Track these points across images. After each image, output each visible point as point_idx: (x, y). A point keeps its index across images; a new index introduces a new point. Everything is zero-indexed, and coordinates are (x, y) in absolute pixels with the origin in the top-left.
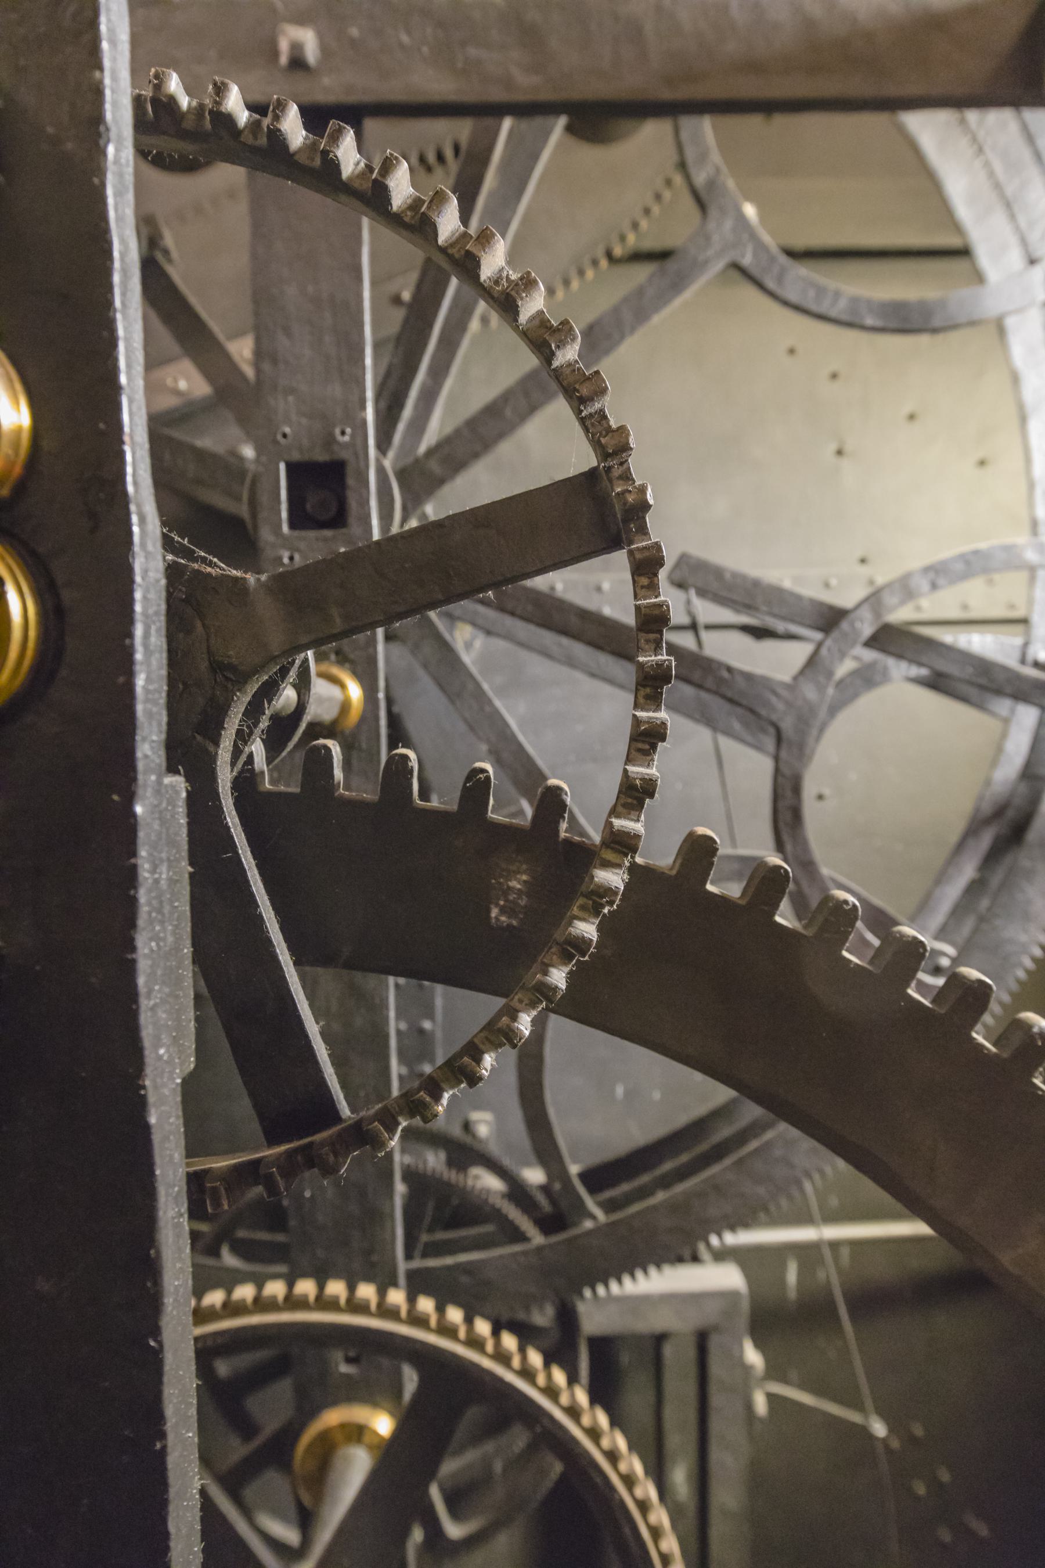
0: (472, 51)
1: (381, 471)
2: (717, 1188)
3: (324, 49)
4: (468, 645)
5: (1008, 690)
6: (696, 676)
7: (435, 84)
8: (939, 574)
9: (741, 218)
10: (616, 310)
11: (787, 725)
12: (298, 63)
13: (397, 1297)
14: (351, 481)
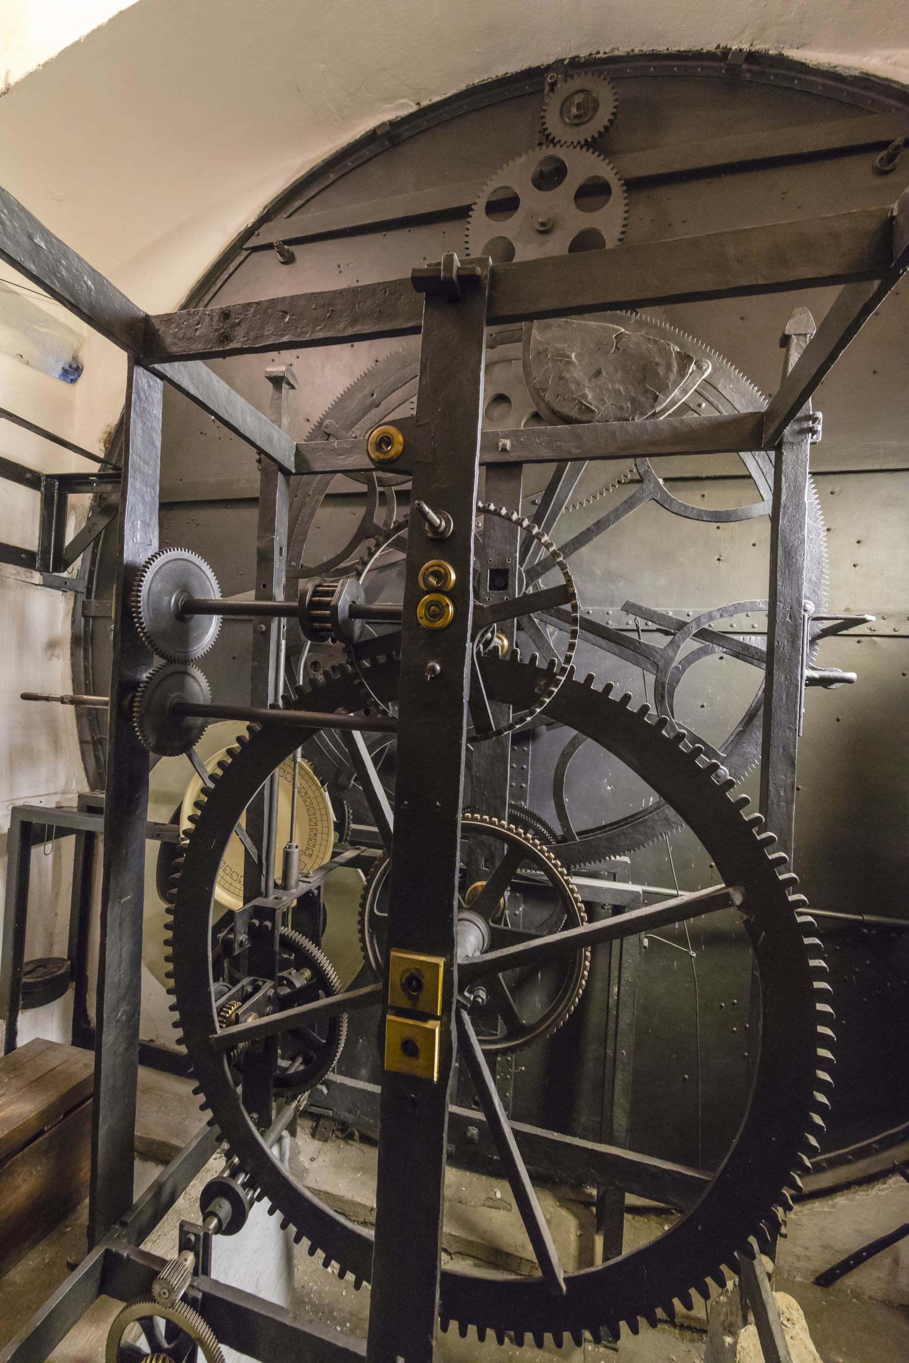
0: (559, 443)
1: (520, 572)
2: (624, 834)
3: (512, 445)
4: (552, 634)
5: (756, 657)
6: (627, 644)
7: (546, 454)
8: (723, 612)
9: (658, 482)
10: (608, 515)
11: (661, 664)
12: (504, 450)
13: (504, 822)
14: (510, 575)
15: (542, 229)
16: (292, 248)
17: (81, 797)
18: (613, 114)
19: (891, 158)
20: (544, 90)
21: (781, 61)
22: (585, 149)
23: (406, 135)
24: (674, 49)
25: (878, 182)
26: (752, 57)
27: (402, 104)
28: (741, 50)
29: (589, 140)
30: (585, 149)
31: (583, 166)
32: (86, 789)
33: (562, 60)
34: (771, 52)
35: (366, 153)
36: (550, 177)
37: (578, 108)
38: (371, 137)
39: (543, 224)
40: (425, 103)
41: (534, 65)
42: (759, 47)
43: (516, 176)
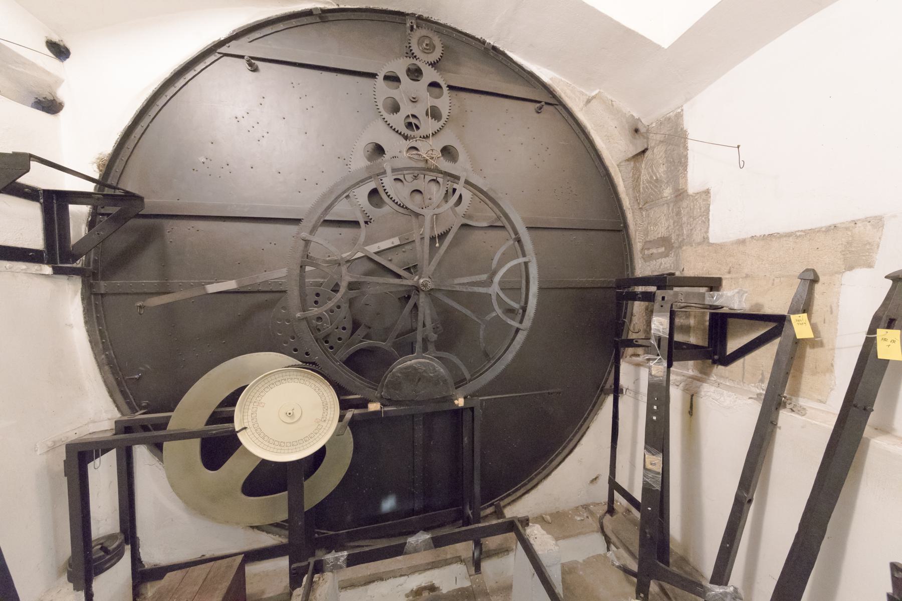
16: (257, 63)
23: (330, 19)
24: (464, 31)
25: (536, 115)
26: (494, 48)
31: (430, 75)
35: (305, 20)
36: (415, 73)
37: (427, 45)
38: (308, 13)
40: (342, 6)
43: (399, 67)
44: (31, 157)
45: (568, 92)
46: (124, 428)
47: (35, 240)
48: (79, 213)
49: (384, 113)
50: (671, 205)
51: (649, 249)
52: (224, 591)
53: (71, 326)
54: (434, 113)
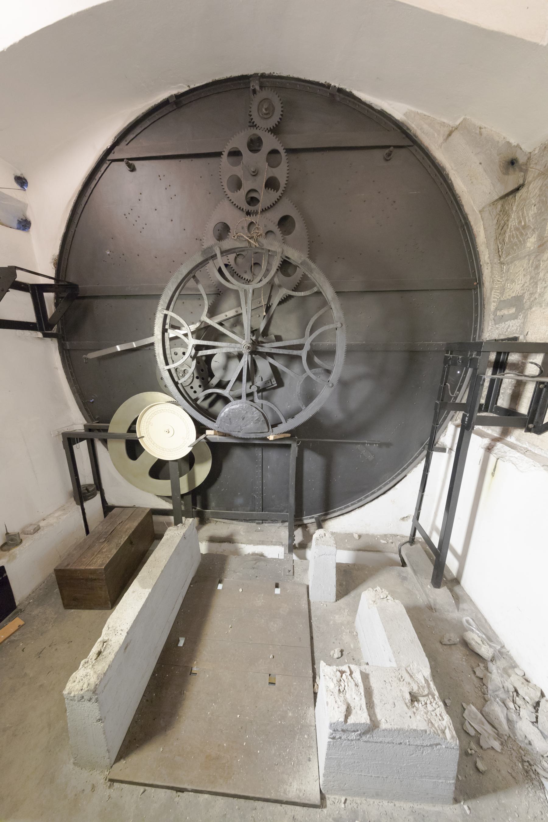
15: (253, 174)
17: (85, 426)
18: (280, 119)
19: (389, 155)
20: (249, 87)
21: (350, 95)
22: (270, 133)
23: (184, 102)
26: (340, 90)
27: (181, 86)
28: (335, 86)
29: (272, 128)
30: (270, 133)
31: (270, 142)
32: (85, 422)
33: (257, 74)
34: (347, 90)
35: (164, 110)
36: (254, 145)
37: (266, 109)
39: (254, 172)
40: (192, 86)
41: (245, 74)
42: (341, 87)
43: (239, 141)
44: (16, 268)
45: (425, 127)
46: (89, 429)
47: (31, 317)
48: (49, 297)
49: (228, 192)
50: (532, 257)
51: (501, 310)
52: (139, 521)
53: (57, 368)
54: (272, 184)
